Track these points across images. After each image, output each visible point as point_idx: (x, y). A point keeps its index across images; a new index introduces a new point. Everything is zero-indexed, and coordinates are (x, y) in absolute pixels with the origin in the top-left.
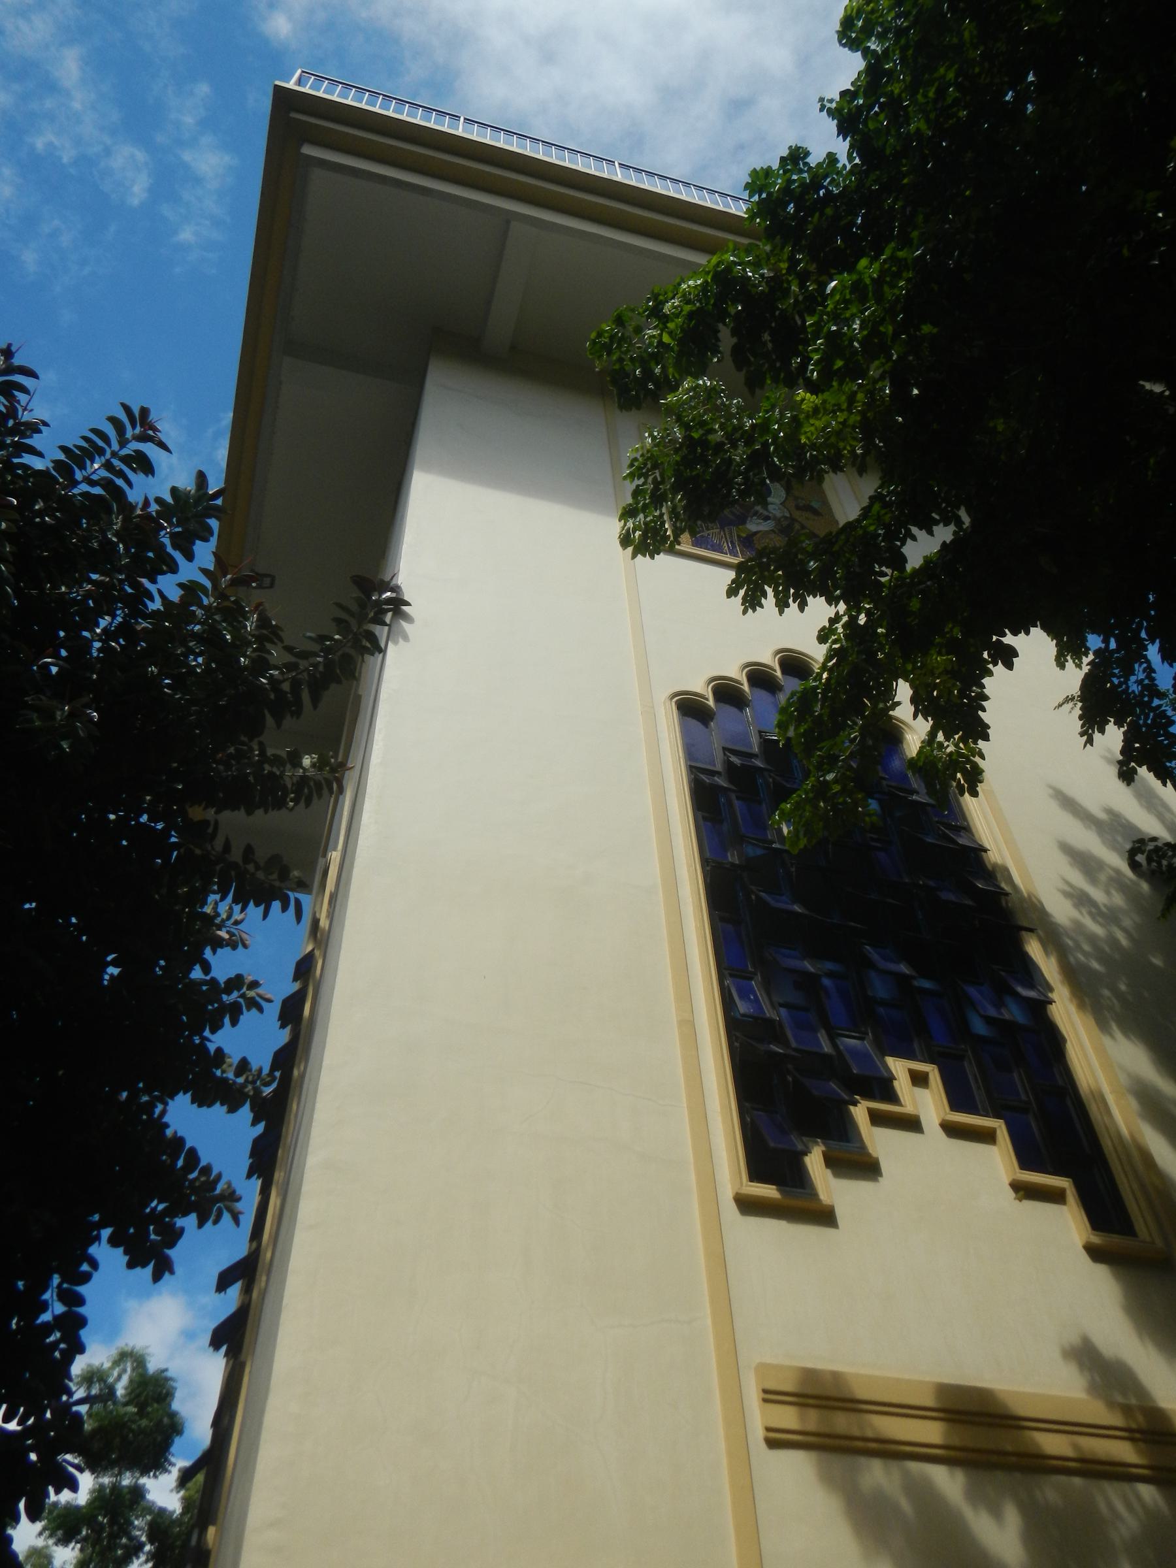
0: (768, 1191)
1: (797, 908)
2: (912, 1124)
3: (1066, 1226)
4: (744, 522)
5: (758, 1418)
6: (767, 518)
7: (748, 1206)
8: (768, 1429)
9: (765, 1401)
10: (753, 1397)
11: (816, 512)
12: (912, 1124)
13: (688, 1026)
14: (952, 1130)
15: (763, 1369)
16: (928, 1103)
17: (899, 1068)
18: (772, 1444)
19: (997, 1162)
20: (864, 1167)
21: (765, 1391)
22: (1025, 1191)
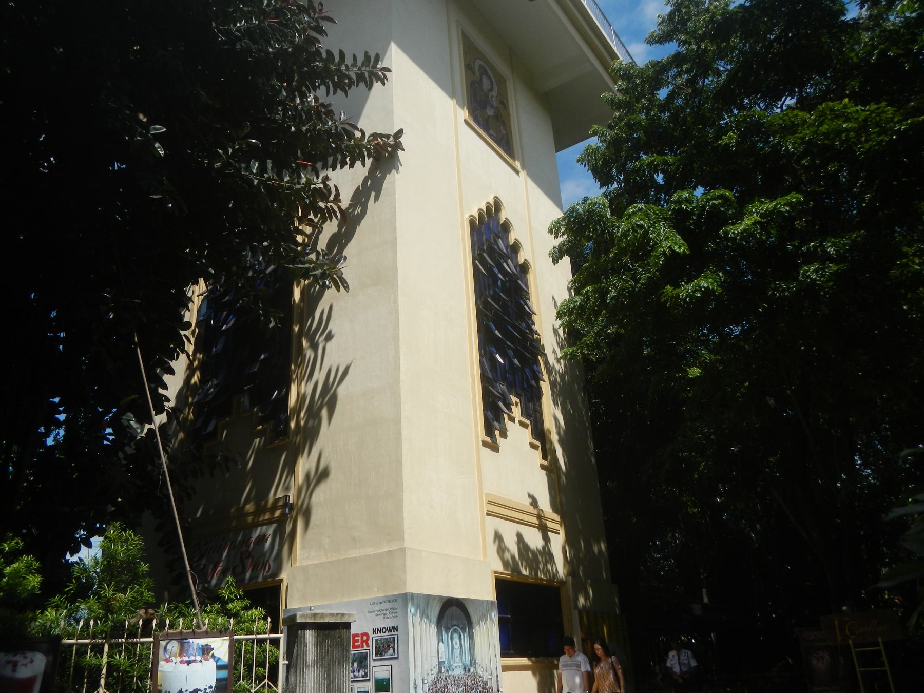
0: (488, 439)
1: (497, 332)
2: (512, 419)
3: (536, 456)
5: (486, 508)
6: (492, 107)
7: (485, 444)
12: (512, 419)
13: (473, 376)
14: (522, 424)
16: (516, 412)
17: (514, 399)
18: (488, 514)
19: (526, 435)
20: (504, 435)
22: (532, 446)
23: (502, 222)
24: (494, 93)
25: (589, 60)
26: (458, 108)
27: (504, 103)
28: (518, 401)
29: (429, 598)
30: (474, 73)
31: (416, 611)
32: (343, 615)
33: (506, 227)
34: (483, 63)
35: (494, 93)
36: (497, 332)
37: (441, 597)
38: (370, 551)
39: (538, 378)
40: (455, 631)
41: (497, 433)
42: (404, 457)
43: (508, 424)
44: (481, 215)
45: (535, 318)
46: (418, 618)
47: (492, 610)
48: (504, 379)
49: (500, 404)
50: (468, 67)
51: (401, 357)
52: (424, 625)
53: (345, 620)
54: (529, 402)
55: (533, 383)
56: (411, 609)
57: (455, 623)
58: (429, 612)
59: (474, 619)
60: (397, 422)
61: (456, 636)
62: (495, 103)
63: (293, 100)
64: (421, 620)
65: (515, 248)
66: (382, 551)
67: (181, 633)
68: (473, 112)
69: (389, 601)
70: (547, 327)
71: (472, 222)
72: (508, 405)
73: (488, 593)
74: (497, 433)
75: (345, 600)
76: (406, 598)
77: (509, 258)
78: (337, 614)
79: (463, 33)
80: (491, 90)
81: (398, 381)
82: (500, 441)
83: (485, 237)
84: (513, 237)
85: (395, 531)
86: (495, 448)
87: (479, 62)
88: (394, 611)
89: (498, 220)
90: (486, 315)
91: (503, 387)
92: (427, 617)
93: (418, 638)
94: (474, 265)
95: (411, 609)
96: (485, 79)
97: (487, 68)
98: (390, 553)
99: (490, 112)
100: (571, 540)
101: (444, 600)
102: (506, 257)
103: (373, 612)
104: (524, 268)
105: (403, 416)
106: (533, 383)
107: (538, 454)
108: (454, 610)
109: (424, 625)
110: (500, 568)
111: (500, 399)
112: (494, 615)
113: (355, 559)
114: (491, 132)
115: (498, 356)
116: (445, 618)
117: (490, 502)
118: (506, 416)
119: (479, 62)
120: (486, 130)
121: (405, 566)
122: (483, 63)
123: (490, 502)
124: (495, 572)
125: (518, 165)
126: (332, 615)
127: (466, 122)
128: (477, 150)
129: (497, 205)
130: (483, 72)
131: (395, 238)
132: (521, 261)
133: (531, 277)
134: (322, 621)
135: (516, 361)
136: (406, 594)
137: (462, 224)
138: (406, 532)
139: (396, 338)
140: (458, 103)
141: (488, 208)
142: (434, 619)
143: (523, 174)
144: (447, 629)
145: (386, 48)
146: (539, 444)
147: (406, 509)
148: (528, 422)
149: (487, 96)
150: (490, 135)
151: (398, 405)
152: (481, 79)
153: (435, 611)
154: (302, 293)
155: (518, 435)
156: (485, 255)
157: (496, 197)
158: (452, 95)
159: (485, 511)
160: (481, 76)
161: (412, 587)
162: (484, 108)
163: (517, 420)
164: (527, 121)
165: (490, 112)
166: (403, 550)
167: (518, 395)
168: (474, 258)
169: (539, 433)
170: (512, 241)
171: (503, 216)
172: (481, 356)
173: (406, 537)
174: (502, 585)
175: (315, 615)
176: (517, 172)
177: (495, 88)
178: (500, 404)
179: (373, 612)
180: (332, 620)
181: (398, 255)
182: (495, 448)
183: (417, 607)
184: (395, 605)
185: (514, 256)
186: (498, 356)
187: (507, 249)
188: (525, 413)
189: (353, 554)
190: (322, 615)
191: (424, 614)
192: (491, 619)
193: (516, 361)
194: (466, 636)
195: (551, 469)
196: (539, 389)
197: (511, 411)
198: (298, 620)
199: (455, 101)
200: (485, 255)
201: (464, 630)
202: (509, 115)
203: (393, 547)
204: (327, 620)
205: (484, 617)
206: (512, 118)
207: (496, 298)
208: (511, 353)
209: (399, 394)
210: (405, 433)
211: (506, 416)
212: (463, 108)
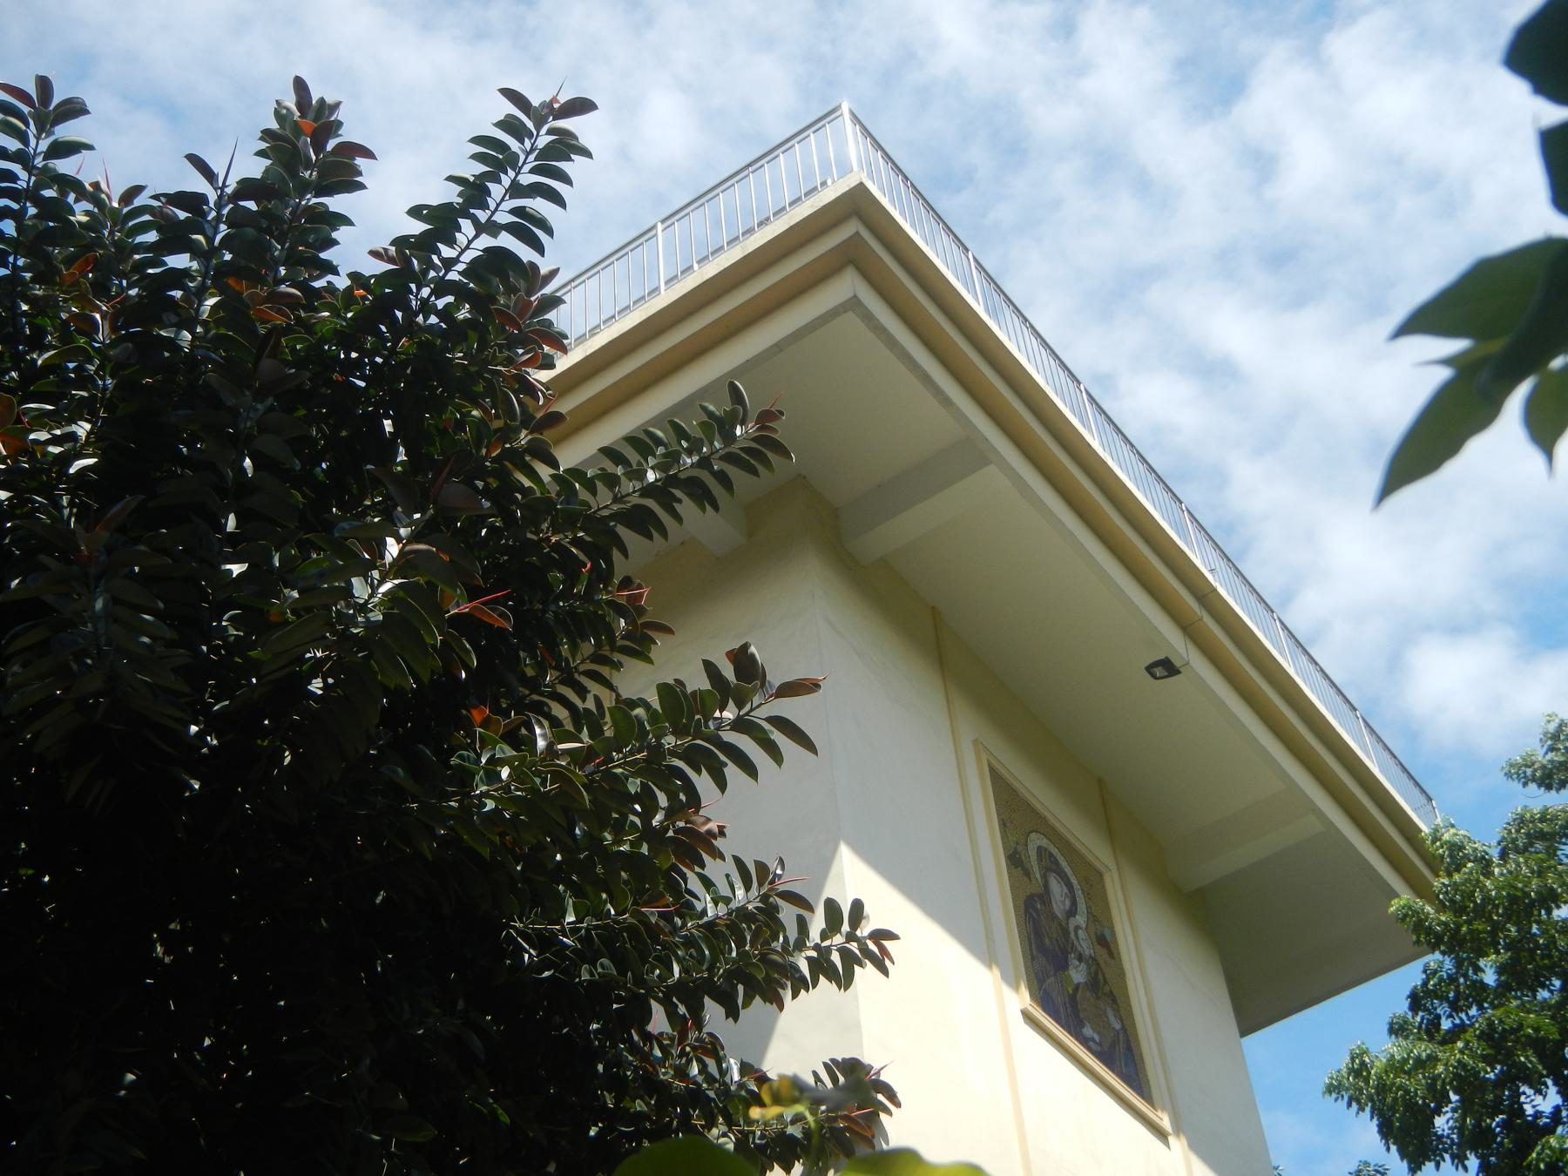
6: (1080, 958)
11: (1111, 954)
24: (1080, 919)
25: (1316, 811)
26: (1007, 992)
27: (1106, 942)
30: (1027, 873)
34: (1044, 842)
50: (1015, 860)
62: (1085, 945)
68: (1043, 997)
79: (992, 770)
80: (1072, 912)
87: (1036, 841)
96: (1056, 888)
97: (1054, 851)
99: (1078, 975)
114: (1088, 1031)
119: (1036, 841)
120: (1075, 1031)
122: (1044, 842)
127: (1028, 1017)
128: (1058, 1088)
130: (1050, 865)
140: (1005, 977)
143: (1178, 1145)
145: (825, 863)
149: (1066, 932)
150: (1084, 1041)
152: (1046, 885)
158: (989, 957)
160: (1044, 877)
162: (1062, 965)
164: (1167, 978)
165: (1078, 975)
176: (1161, 1134)
177: (1082, 905)
199: (996, 971)
206: (1129, 975)
212: (1016, 988)
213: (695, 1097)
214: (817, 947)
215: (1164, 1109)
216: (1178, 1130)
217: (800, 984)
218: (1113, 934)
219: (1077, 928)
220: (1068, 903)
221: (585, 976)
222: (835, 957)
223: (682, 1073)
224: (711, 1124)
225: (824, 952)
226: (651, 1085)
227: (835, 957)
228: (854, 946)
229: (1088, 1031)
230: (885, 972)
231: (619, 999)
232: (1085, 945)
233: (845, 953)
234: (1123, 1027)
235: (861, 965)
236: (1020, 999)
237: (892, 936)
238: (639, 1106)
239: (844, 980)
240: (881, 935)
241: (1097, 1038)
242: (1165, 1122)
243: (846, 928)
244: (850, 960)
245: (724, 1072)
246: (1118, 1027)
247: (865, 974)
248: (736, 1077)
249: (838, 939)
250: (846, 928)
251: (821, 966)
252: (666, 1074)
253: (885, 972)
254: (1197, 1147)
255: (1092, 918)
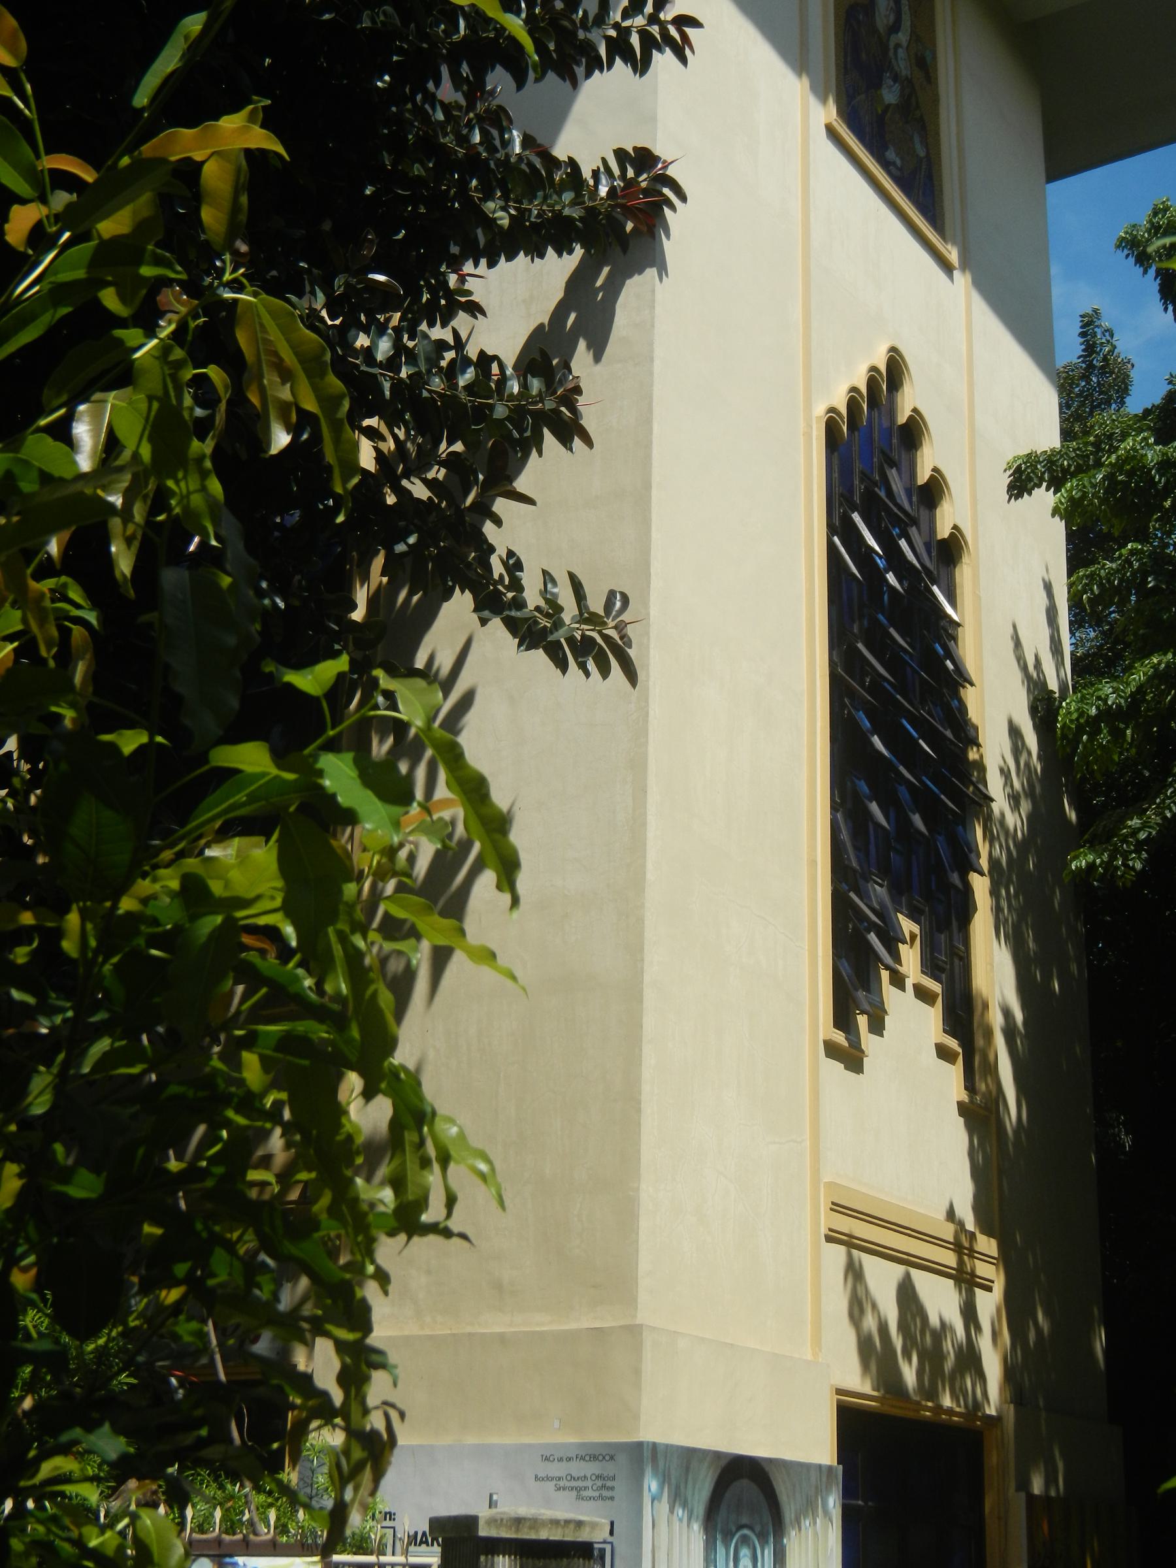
0: (840, 1038)
2: (898, 981)
3: (950, 1082)
4: (879, 86)
6: (896, 78)
7: (832, 1050)
8: (830, 1230)
9: (832, 1209)
10: (824, 1206)
12: (898, 981)
13: (813, 863)
14: (922, 994)
15: (831, 1185)
16: (910, 959)
17: (907, 926)
18: (829, 1239)
21: (833, 1203)
22: (943, 1053)
23: (902, 419)
24: (902, 37)
26: (813, 101)
27: (925, 65)
28: (916, 929)
29: (690, 1456)
31: (661, 1487)
32: (579, 1524)
33: (912, 434)
35: (902, 37)
36: (876, 740)
37: (718, 1455)
38: (544, 1323)
39: (965, 863)
40: (745, 1540)
41: (862, 1021)
42: (646, 1088)
43: (889, 992)
44: (853, 404)
45: (970, 696)
46: (664, 1506)
47: (828, 1490)
48: (885, 871)
49: (872, 937)
51: (651, 819)
52: (676, 1525)
53: (584, 1536)
54: (940, 931)
55: (955, 878)
56: (651, 1484)
57: (745, 1520)
58: (689, 1493)
59: (788, 1513)
60: (633, 993)
61: (745, 1552)
62: (903, 65)
63: (515, 208)
64: (672, 1511)
65: (932, 493)
66: (573, 1326)
67: (219, 1542)
68: (850, 113)
69: (594, 1458)
70: (997, 709)
71: (831, 428)
72: (892, 940)
73: (813, 1443)
74: (862, 1021)
75: (471, 1440)
76: (641, 1455)
77: (915, 522)
78: (567, 1522)
80: (895, 28)
81: (638, 882)
82: (868, 1041)
83: (858, 466)
84: (927, 462)
85: (615, 1280)
86: (852, 1059)
88: (605, 1484)
89: (892, 412)
90: (852, 694)
91: (879, 891)
92: (684, 1505)
93: (662, 1556)
94: (831, 549)
95: (651, 1484)
98: (598, 1333)
99: (890, 95)
100: (1016, 1307)
101: (723, 1463)
102: (905, 523)
103: (548, 1479)
104: (950, 551)
105: (647, 978)
106: (955, 878)
107: (954, 1074)
108: (744, 1487)
109: (676, 1525)
110: (856, 1380)
111: (872, 926)
112: (833, 1502)
113: (502, 1339)
114: (891, 155)
115: (874, 807)
116: (723, 1507)
117: (837, 1208)
118: (885, 975)
121: (637, 1372)
123: (837, 1208)
124: (839, 1392)
125: (953, 255)
126: (555, 1523)
127: (831, 131)
129: (894, 372)
131: (647, 486)
132: (943, 531)
133: (965, 574)
134: (533, 1536)
135: (917, 820)
136: (640, 1445)
137: (808, 436)
138: (644, 1283)
139: (638, 765)
140: (814, 88)
141: (872, 383)
142: (700, 1509)
143: (962, 280)
144: (728, 1536)
146: (953, 1044)
147: (644, 1224)
148: (936, 987)
151: (635, 951)
153: (701, 1491)
154: (372, 602)
155: (911, 1021)
156: (856, 517)
157: (893, 349)
158: (799, 63)
159: (823, 1231)
161: (652, 1432)
162: (875, 84)
163: (909, 983)
164: (981, 109)
165: (890, 95)
166: (634, 1331)
167: (913, 916)
168: (832, 529)
169: (961, 1014)
170: (923, 475)
171: (908, 401)
172: (834, 808)
173: (643, 1297)
174: (853, 1423)
175: (518, 1521)
176: (947, 268)
178: (872, 937)
179: (548, 1479)
180: (556, 1535)
181: (655, 535)
182: (852, 1059)
183: (664, 1479)
184: (609, 1468)
185: (924, 514)
186: (874, 807)
187: (909, 492)
188: (931, 966)
189: (495, 1324)
190: (535, 1523)
191: (678, 1497)
192: (826, 1513)
193: (917, 820)
194: (769, 1553)
195: (979, 1114)
196: (967, 891)
197: (897, 958)
198: (483, 1532)
199: (806, 81)
200: (856, 517)
201: (763, 1537)
202: (936, 101)
203: (606, 1319)
204: (544, 1535)
205: (809, 1507)
207: (880, 645)
208: (903, 793)
209: (641, 920)
210: (649, 1022)
211: (885, 975)
212: (824, 101)
213: (473, 164)
214: (616, 26)
215: (954, 243)
216: (965, 265)
217: (595, 65)
218: (934, 57)
219: (898, 46)
220: (892, 18)
221: (366, 23)
222: (635, 40)
223: (464, 140)
224: (488, 196)
225: (624, 33)
226: (429, 146)
227: (635, 40)
228: (655, 30)
229: (891, 155)
230: (684, 60)
231: (400, 51)
232: (903, 65)
233: (644, 35)
234: (928, 153)
235: (660, 50)
236: (826, 113)
237: (694, 23)
238: (417, 170)
239: (641, 66)
240: (684, 21)
241: (898, 162)
242: (953, 255)
243: (649, 9)
244: (649, 43)
245: (507, 144)
246: (922, 153)
247: (663, 60)
248: (518, 150)
249: (639, 21)
250: (649, 9)
251: (619, 47)
252: (448, 140)
253: (684, 60)
254: (980, 284)
255: (915, 37)
